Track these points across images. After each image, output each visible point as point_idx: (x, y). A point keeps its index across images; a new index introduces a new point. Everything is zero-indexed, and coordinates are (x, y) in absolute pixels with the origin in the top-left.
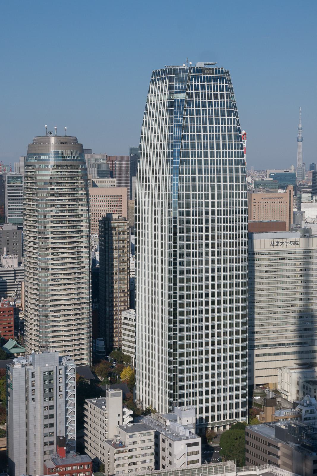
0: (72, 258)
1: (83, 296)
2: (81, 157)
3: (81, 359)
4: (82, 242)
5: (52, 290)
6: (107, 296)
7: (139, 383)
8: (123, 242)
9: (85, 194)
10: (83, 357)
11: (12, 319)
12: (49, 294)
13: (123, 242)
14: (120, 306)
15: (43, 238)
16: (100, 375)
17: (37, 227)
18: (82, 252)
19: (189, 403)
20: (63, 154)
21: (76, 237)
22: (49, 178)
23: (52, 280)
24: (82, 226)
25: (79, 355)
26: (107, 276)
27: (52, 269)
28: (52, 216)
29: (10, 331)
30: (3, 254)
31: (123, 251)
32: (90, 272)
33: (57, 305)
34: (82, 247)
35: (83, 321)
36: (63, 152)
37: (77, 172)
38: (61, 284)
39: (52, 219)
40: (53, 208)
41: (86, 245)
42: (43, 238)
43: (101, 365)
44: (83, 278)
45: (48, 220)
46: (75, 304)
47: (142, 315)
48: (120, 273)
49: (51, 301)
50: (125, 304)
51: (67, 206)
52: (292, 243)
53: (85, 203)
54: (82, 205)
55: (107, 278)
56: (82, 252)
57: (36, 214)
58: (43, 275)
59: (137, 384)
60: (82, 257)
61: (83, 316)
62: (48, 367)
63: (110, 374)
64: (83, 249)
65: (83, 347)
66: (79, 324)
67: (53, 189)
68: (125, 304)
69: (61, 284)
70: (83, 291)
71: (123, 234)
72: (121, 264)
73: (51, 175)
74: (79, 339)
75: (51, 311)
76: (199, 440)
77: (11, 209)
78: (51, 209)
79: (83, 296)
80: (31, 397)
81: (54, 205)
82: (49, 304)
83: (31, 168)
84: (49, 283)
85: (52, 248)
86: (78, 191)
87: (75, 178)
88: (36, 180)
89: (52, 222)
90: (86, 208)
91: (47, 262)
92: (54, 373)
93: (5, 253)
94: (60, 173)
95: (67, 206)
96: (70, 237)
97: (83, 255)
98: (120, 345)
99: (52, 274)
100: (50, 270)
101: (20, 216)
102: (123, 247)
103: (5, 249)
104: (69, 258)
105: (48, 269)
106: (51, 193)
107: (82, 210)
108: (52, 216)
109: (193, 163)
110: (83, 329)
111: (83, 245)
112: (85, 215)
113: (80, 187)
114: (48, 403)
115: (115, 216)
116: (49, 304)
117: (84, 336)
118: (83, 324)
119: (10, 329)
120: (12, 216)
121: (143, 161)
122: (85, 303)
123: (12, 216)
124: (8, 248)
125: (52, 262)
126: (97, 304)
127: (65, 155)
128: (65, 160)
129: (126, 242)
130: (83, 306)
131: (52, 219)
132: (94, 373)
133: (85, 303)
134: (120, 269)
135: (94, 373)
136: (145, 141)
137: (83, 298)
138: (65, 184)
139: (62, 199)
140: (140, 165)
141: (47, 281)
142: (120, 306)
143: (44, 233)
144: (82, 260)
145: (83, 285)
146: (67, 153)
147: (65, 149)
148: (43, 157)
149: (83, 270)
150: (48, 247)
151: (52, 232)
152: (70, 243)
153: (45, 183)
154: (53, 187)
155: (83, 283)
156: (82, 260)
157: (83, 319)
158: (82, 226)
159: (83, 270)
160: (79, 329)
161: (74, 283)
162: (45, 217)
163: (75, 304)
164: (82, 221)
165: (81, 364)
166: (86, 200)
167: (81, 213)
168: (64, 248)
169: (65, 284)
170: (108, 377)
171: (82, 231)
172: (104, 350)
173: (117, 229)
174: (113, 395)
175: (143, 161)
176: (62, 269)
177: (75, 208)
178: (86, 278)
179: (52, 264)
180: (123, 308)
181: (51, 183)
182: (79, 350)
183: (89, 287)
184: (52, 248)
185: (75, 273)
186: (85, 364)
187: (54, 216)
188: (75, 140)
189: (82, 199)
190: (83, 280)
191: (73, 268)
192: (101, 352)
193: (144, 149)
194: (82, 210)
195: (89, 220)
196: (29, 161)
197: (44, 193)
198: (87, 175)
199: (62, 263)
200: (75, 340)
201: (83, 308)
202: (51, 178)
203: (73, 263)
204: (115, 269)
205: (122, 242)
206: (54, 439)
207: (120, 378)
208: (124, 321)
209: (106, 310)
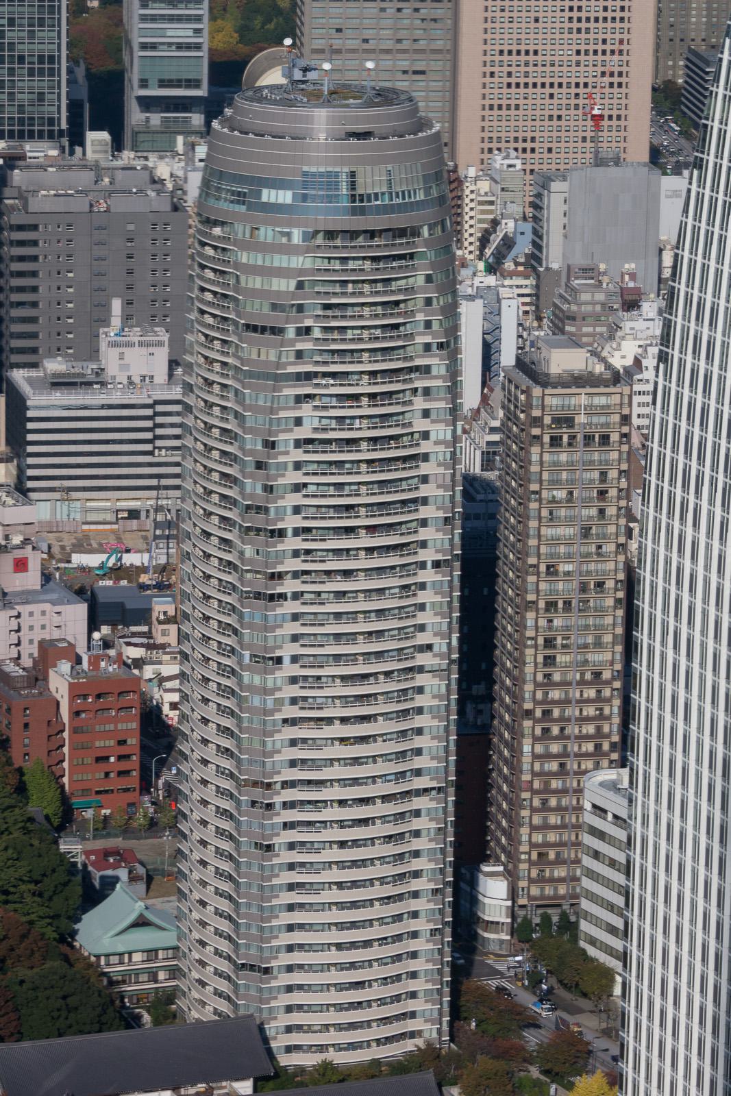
0: (380, 613)
3: (404, 1016)
4: (423, 544)
5: (293, 743)
8: (603, 474)
9: (441, 346)
10: (411, 1005)
11: (135, 725)
12: (277, 758)
13: (603, 474)
14: (582, 738)
15: (258, 530)
17: (235, 480)
20: (353, 185)
22: (293, 284)
23: (294, 701)
24: (425, 479)
27: (295, 659)
29: (121, 773)
30: (105, 322)
31: (602, 512)
32: (452, 662)
33: (310, 823)
34: (423, 565)
35: (416, 864)
36: (353, 174)
37: (412, 256)
38: (329, 721)
40: (306, 410)
41: (439, 557)
44: (420, 690)
45: (282, 459)
49: (285, 785)
50: (599, 729)
51: (364, 445)
53: (439, 383)
54: (427, 391)
56: (422, 586)
58: (257, 680)
60: (422, 607)
61: (416, 844)
65: (413, 965)
67: (308, 330)
69: (329, 721)
70: (418, 742)
71: (605, 439)
72: (592, 567)
73: (301, 272)
77: (153, 19)
78: (297, 414)
79: (418, 762)
81: (308, 396)
83: (217, 231)
84: (279, 716)
85: (296, 575)
86: (411, 336)
88: (237, 289)
89: (298, 466)
90: (442, 404)
91: (273, 629)
93: (116, 322)
95: (365, 401)
96: (371, 529)
97: (422, 597)
99: (294, 680)
100: (286, 660)
101: (188, 47)
102: (602, 493)
103: (117, 305)
105: (279, 660)
106: (299, 346)
107: (426, 414)
110: (415, 894)
113: (420, 317)
116: (279, 820)
119: (124, 765)
120: (153, 47)
123: (153, 47)
124: (129, 303)
127: (360, 191)
128: (362, 211)
129: (613, 474)
131: (299, 455)
134: (584, 588)
137: (418, 772)
139: (346, 374)
141: (270, 704)
143: (267, 510)
144: (421, 618)
146: (372, 181)
148: (268, 196)
149: (423, 659)
150: (280, 569)
151: (297, 510)
152: (370, 550)
153: (274, 307)
154: (308, 323)
155: (420, 711)
156: (421, 618)
158: (425, 479)
159: (423, 659)
160: (400, 897)
162: (271, 445)
164: (426, 457)
166: (443, 371)
167: (420, 425)
168: (347, 573)
169: (344, 720)
173: (581, 419)
176: (337, 657)
177: (399, 409)
179: (295, 638)
181: (300, 308)
184: (296, 575)
185: (388, 674)
187: (309, 441)
189: (427, 369)
190: (420, 701)
191: (379, 654)
194: (426, 414)
196: (212, 202)
197: (268, 345)
199: (338, 636)
200: (383, 941)
202: (300, 285)
203: (380, 633)
208: (590, 819)
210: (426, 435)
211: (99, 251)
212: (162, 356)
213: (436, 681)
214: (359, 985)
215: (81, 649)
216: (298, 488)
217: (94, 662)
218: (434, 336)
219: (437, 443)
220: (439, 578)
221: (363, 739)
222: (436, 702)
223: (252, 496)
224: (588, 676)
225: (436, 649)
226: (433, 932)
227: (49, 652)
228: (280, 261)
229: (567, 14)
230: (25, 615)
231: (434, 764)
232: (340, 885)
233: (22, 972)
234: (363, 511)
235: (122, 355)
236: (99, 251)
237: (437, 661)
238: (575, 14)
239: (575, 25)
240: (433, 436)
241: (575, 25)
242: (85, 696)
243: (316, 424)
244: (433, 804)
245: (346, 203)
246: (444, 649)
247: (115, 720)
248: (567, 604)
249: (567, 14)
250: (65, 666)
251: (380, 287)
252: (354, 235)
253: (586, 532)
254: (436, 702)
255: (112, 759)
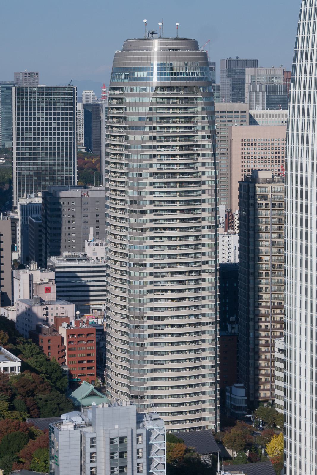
0: (186, 246)
1: (204, 311)
2: (202, 74)
3: (200, 419)
4: (204, 219)
5: (152, 300)
6: (251, 312)
7: (291, 463)
8: (280, 220)
9: (209, 137)
10: (204, 415)
11: (94, 348)
12: (145, 306)
13: (280, 220)
14: (274, 329)
15: (136, 211)
16: (232, 447)
18: (204, 236)
20: (171, 69)
21: (194, 210)
22: (148, 109)
23: (152, 283)
24: (203, 192)
25: (197, 411)
26: (251, 278)
27: (152, 265)
28: (151, 175)
29: (89, 368)
31: (280, 235)
32: (216, 270)
33: (159, 326)
34: (203, 228)
35: (204, 354)
36: (171, 64)
37: (196, 99)
38: (166, 291)
39: (152, 180)
40: (154, 161)
41: (210, 224)
42: (136, 211)
43: (234, 431)
44: (204, 280)
45: (144, 181)
46: (190, 325)
47: (296, 347)
48: (273, 273)
49: (149, 318)
53: (208, 152)
54: (203, 155)
55: (252, 282)
56: (204, 236)
57: (125, 170)
59: (287, 464)
60: (204, 245)
61: (204, 346)
62: (117, 430)
63: (248, 446)
64: (206, 232)
65: (204, 398)
66: (198, 359)
67: (154, 128)
68: (281, 326)
69: (166, 291)
70: (203, 302)
72: (277, 258)
73: (152, 104)
74: (197, 385)
75: (149, 336)
78: (151, 162)
79: (204, 311)
81: (155, 156)
82: (146, 324)
83: (117, 92)
84: (146, 289)
85: (151, 229)
87: (192, 110)
89: (151, 184)
90: (210, 161)
91: (142, 252)
92: (128, 441)
93: (91, 236)
94: (166, 101)
95: (178, 157)
96: (182, 211)
97: (204, 241)
98: (273, 396)
99: (151, 274)
100: (148, 265)
103: (92, 230)
104: (180, 246)
105: (145, 265)
107: (203, 164)
108: (151, 175)
110: (204, 367)
111: (205, 223)
112: (210, 172)
113: (200, 124)
115: (262, 175)
116: (146, 324)
117: (206, 380)
118: (205, 358)
119: (90, 365)
121: (300, 80)
122: (207, 324)
124: (97, 228)
125: (152, 252)
126: (236, 326)
127: (174, 71)
128: (175, 79)
130: (205, 328)
131: (152, 180)
132: (220, 443)
133: (207, 324)
134: (273, 266)
135: (220, 443)
136: (302, 46)
137: (204, 315)
138: (174, 120)
140: (295, 87)
141: (142, 284)
142: (274, 329)
143: (138, 203)
144: (203, 250)
145: (203, 293)
146: (178, 67)
147: (175, 59)
148: (137, 74)
149: (204, 267)
150: (145, 227)
151: (151, 202)
152: (182, 220)
153: (140, 119)
154: (154, 125)
155: (204, 289)
156: (203, 250)
157: (204, 350)
158: (203, 192)
159: (204, 267)
160: (197, 368)
161: (189, 289)
162: (140, 175)
163: (190, 325)
164: (204, 182)
165: (200, 428)
166: (210, 147)
167: (201, 169)
168: (172, 229)
169: (173, 291)
170: (245, 451)
171: (204, 201)
172: (244, 405)
173: (269, 197)
175: (300, 80)
177: (192, 161)
178: (209, 281)
179: (152, 256)
180: (278, 334)
181: (151, 119)
182: (197, 402)
183: (216, 296)
184: (151, 229)
185: (190, 272)
186: (207, 427)
187: (156, 174)
188: (194, 44)
189: (203, 146)
190: (203, 285)
192: (240, 408)
193: (301, 60)
194: (203, 164)
195: (215, 182)
196: (116, 81)
197: (138, 134)
198: (213, 104)
199: (169, 255)
200: (191, 386)
201: (204, 332)
202: (151, 109)
203: (187, 254)
204: (263, 267)
205: (277, 219)
207: (266, 454)
209: (248, 335)
210: (203, 173)
211: (85, 213)
213: (210, 277)
214: (181, 404)
215: (72, 320)
216: (151, 193)
217: (77, 323)
218: (206, 132)
219: (208, 177)
220: (210, 233)
221: (181, 299)
222: (210, 286)
223: (132, 197)
224: (276, 304)
225: (210, 263)
226: (212, 384)
227: (59, 320)
228: (142, 100)
229: (274, 155)
230: (50, 309)
231: (210, 312)
232: (172, 361)
233: (41, 396)
234: (178, 203)
235: (94, 249)
236: (85, 213)
237: (210, 268)
238: (278, 155)
239: (278, 159)
240: (206, 174)
241: (278, 159)
242: (73, 335)
243: (158, 166)
244: (210, 329)
245: (169, 76)
246: (213, 263)
247: (86, 345)
248: (267, 274)
249: (274, 155)
250: (65, 325)
251: (183, 111)
252: (171, 88)
253: (273, 243)
254: (210, 286)
255: (85, 362)
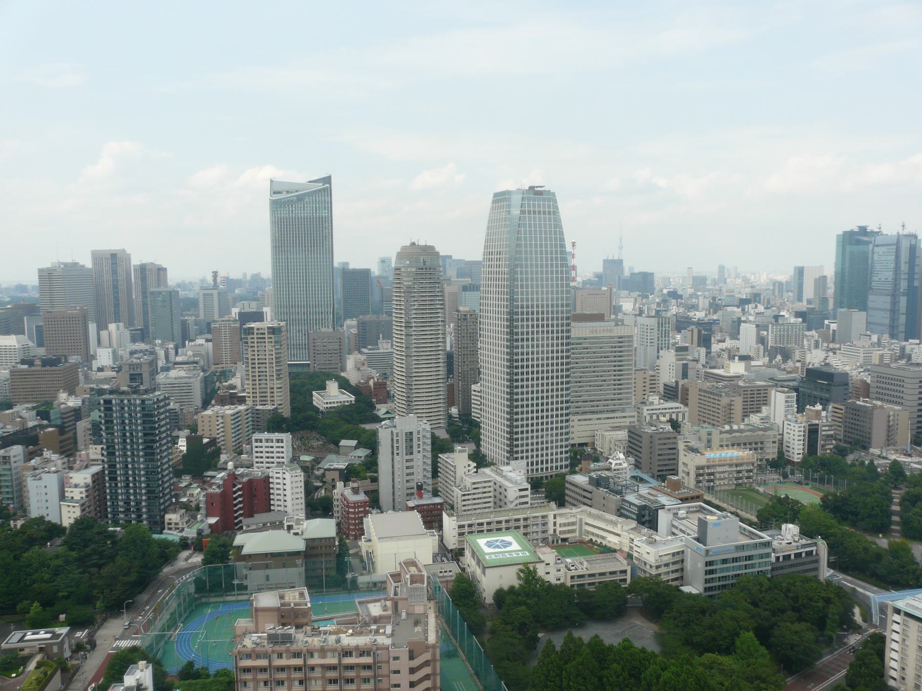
19: (522, 458)
52: (607, 331)
76: (529, 486)
80: (395, 452)
109: (526, 266)
114: (408, 457)
174: (460, 451)
206: (414, 485)
212: (390, 345)
